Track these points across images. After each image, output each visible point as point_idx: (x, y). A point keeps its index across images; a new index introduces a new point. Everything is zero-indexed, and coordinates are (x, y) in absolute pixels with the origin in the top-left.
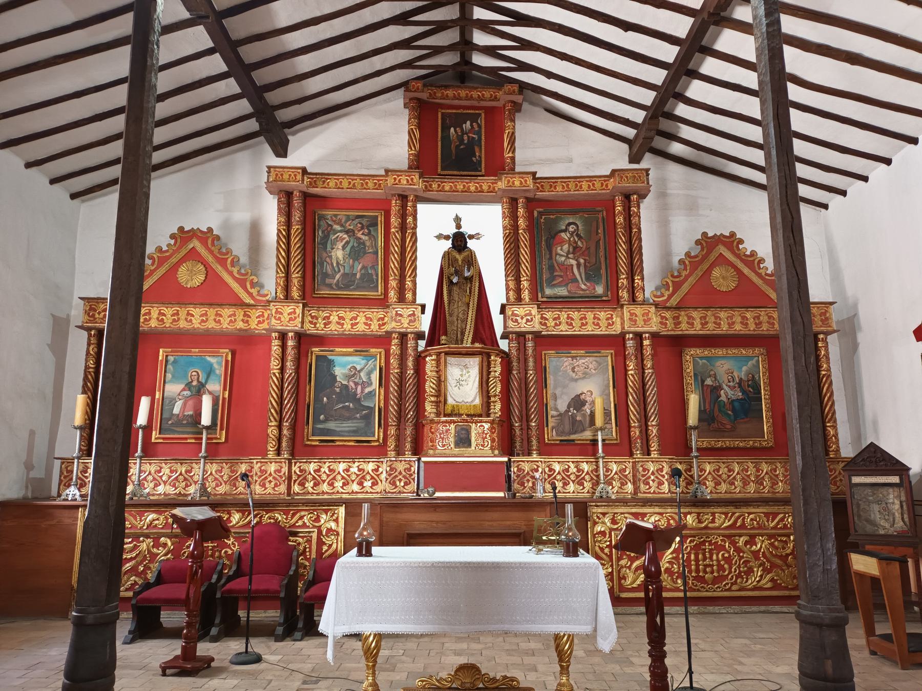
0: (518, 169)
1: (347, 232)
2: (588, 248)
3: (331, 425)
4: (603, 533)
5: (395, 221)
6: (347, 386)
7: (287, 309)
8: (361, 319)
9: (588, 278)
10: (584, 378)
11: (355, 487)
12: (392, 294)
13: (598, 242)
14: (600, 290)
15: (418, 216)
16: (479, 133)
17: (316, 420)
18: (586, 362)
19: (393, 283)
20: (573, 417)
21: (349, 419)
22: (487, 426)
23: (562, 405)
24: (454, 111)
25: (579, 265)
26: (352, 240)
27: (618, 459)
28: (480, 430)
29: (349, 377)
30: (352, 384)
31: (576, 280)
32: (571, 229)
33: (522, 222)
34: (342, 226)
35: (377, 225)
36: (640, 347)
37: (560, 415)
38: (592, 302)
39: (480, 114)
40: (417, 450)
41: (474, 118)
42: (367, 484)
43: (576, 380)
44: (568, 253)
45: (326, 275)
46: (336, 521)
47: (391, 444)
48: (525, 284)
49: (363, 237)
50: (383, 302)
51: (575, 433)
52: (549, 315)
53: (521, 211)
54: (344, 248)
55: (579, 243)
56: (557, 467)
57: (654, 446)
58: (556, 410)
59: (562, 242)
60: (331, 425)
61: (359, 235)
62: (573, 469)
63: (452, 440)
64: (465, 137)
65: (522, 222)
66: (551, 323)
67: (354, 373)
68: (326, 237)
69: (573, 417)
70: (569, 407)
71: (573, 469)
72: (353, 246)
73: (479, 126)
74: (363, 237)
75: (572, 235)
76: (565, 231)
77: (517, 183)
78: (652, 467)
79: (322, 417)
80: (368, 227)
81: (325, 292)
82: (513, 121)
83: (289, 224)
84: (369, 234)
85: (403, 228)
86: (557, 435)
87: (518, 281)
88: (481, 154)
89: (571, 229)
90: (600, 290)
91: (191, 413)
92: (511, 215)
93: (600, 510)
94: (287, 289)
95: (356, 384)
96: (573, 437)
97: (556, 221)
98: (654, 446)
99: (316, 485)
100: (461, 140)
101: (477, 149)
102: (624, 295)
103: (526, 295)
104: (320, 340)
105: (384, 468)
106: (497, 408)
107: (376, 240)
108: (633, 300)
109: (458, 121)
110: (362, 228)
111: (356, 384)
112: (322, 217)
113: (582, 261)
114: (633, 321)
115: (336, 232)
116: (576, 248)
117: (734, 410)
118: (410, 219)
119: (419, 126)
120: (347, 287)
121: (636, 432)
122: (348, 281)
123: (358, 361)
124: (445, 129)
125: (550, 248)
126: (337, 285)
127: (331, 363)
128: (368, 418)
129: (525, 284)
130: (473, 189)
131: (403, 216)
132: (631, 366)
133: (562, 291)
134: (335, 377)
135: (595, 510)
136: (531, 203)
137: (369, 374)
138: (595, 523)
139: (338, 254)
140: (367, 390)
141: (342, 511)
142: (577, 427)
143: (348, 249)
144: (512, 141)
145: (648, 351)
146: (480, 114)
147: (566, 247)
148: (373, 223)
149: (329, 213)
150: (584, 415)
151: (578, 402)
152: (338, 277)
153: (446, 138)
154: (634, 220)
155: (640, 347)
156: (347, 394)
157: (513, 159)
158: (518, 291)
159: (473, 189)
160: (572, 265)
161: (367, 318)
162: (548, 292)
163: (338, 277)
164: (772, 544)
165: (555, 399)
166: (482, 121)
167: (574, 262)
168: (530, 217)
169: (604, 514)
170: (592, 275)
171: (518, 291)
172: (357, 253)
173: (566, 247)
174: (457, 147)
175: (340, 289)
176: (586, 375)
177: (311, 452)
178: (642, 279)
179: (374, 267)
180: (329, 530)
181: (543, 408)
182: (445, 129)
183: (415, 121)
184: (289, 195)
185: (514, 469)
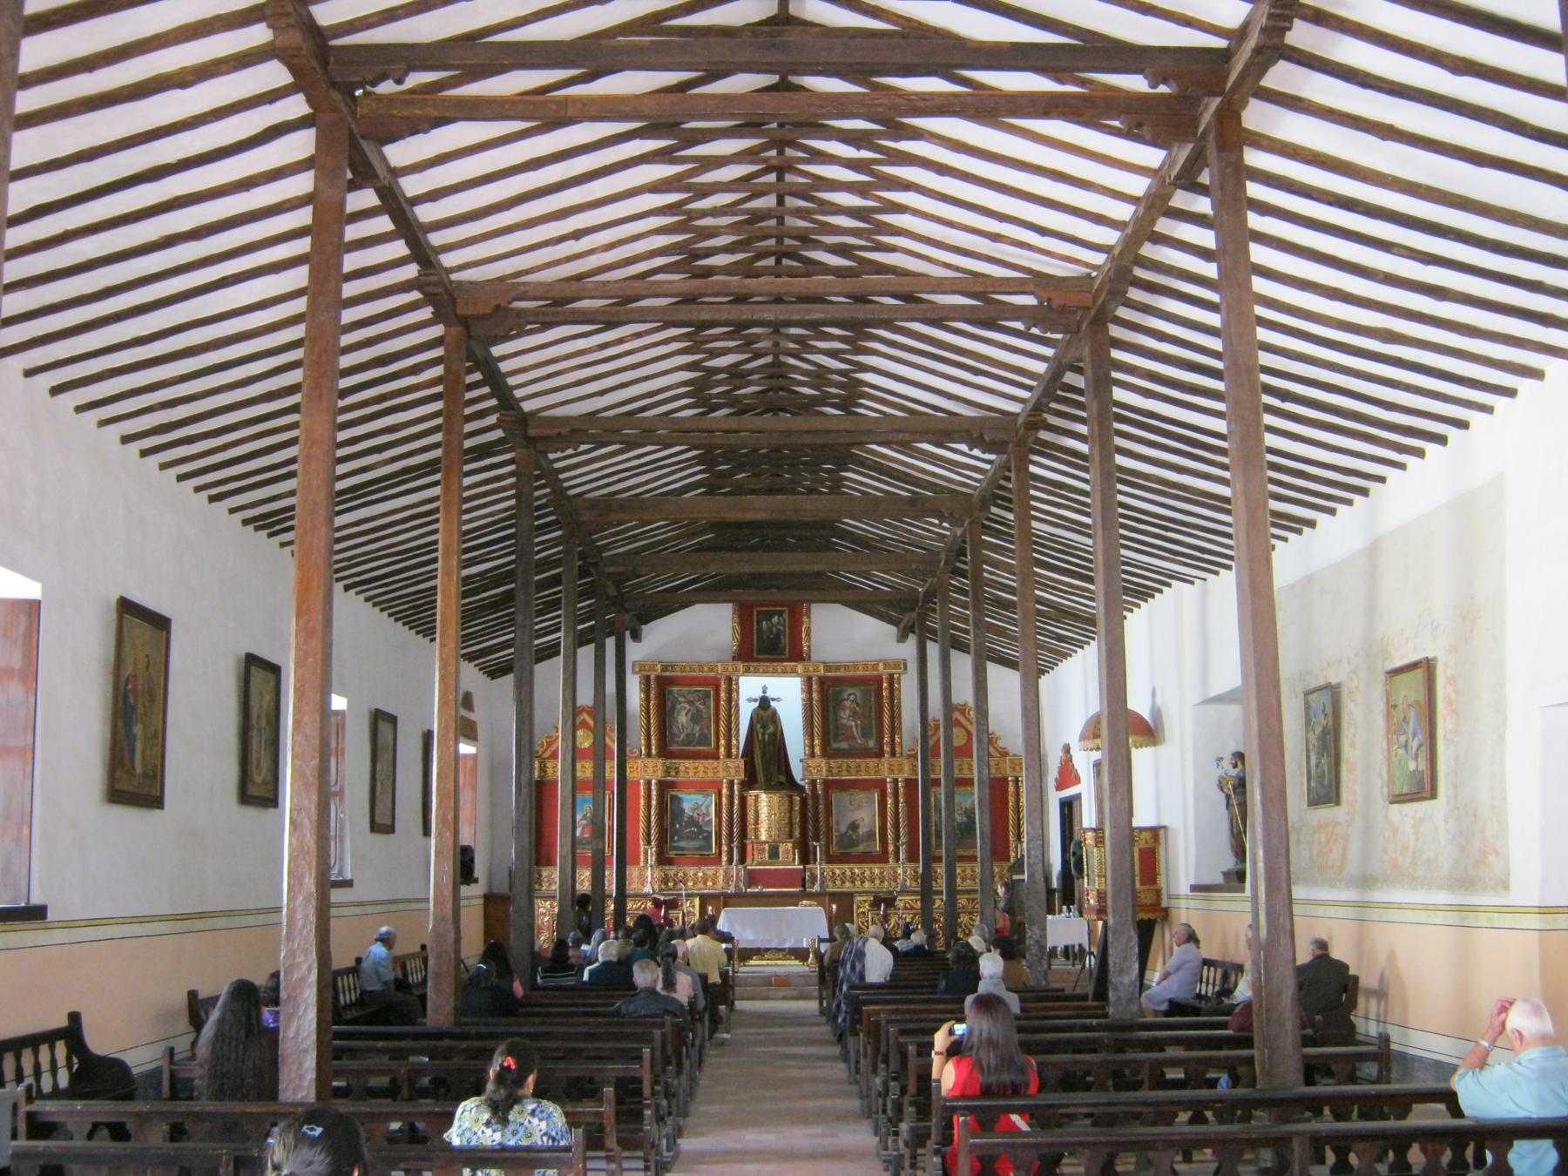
0: (812, 659)
1: (690, 702)
2: (863, 713)
3: (682, 844)
4: (863, 913)
5: (723, 695)
6: (692, 817)
7: (650, 762)
8: (701, 769)
9: (863, 736)
10: (858, 809)
11: (700, 885)
12: (722, 750)
13: (871, 708)
14: (871, 744)
15: (740, 691)
16: (784, 626)
17: (672, 840)
18: (860, 796)
19: (722, 742)
20: (850, 836)
21: (694, 839)
22: (790, 845)
23: (843, 828)
24: (766, 609)
25: (856, 726)
26: (692, 708)
27: (879, 865)
28: (786, 847)
29: (694, 810)
30: (696, 815)
31: (853, 737)
32: (852, 697)
33: (815, 695)
34: (684, 697)
35: (709, 697)
36: (896, 789)
37: (841, 835)
38: (865, 753)
39: (784, 611)
40: (742, 860)
41: (780, 614)
42: (710, 884)
43: (852, 810)
44: (849, 716)
45: (675, 735)
46: (693, 907)
47: (724, 858)
48: (817, 742)
49: (701, 707)
50: (716, 757)
51: (851, 847)
52: (833, 763)
53: (815, 687)
54: (686, 714)
55: (857, 709)
56: (838, 872)
57: (902, 856)
58: (838, 830)
59: (844, 708)
60: (682, 844)
61: (698, 704)
62: (848, 873)
63: (767, 855)
64: (774, 629)
65: (815, 695)
66: (835, 771)
67: (697, 807)
68: (674, 707)
69: (850, 836)
70: (848, 829)
71: (848, 873)
72: (693, 714)
73: (784, 620)
74: (701, 707)
75: (852, 702)
76: (847, 699)
77: (811, 669)
78: (900, 871)
79: (676, 838)
80: (704, 699)
81: (674, 748)
82: (809, 617)
83: (648, 699)
84: (704, 704)
85: (729, 700)
86: (840, 849)
87: (812, 740)
88: (785, 641)
89: (852, 697)
90: (871, 744)
91: (587, 835)
92: (808, 690)
93: (862, 898)
94: (648, 747)
95: (699, 815)
96: (850, 850)
97: (842, 691)
98: (902, 856)
99: (675, 884)
100: (771, 632)
101: (782, 637)
102: (887, 748)
103: (817, 750)
104: (672, 785)
105: (721, 873)
106: (797, 833)
107: (709, 708)
108: (893, 754)
109: (768, 616)
110: (699, 700)
111: (699, 815)
112: (670, 692)
113: (859, 722)
114: (891, 770)
115: (680, 703)
116: (855, 713)
117: (960, 830)
118: (734, 694)
119: (741, 624)
120: (689, 744)
121: (891, 848)
122: (690, 740)
123: (699, 798)
124: (759, 623)
125: (836, 714)
126: (682, 741)
127: (679, 800)
128: (708, 838)
129: (817, 742)
130: (780, 670)
131: (729, 691)
132: (890, 801)
133: (844, 745)
134: (683, 811)
135: (859, 898)
136: (823, 681)
137: (708, 807)
138: (859, 907)
139: (683, 719)
140: (706, 819)
141: (697, 901)
142: (854, 843)
143: (690, 714)
144: (808, 634)
145: (901, 790)
146: (784, 611)
147: (848, 712)
148: (707, 695)
149: (676, 689)
150: (858, 835)
151: (854, 826)
152: (682, 736)
153: (760, 629)
154: (896, 693)
155: (896, 789)
156: (692, 822)
157: (809, 647)
158: (812, 747)
159: (780, 670)
160: (851, 727)
161: (705, 768)
162: (835, 745)
163: (682, 736)
164: (971, 919)
165: (838, 823)
166: (786, 616)
167: (853, 723)
168: (822, 691)
169: (865, 901)
170: (866, 734)
171: (812, 747)
172: (696, 718)
173: (848, 712)
174: (768, 637)
175: (684, 745)
176: (860, 807)
177: (670, 862)
178: (901, 738)
179: (709, 729)
180: (689, 912)
181: (829, 829)
182: (759, 623)
183: (736, 619)
184: (647, 678)
185: (808, 874)
